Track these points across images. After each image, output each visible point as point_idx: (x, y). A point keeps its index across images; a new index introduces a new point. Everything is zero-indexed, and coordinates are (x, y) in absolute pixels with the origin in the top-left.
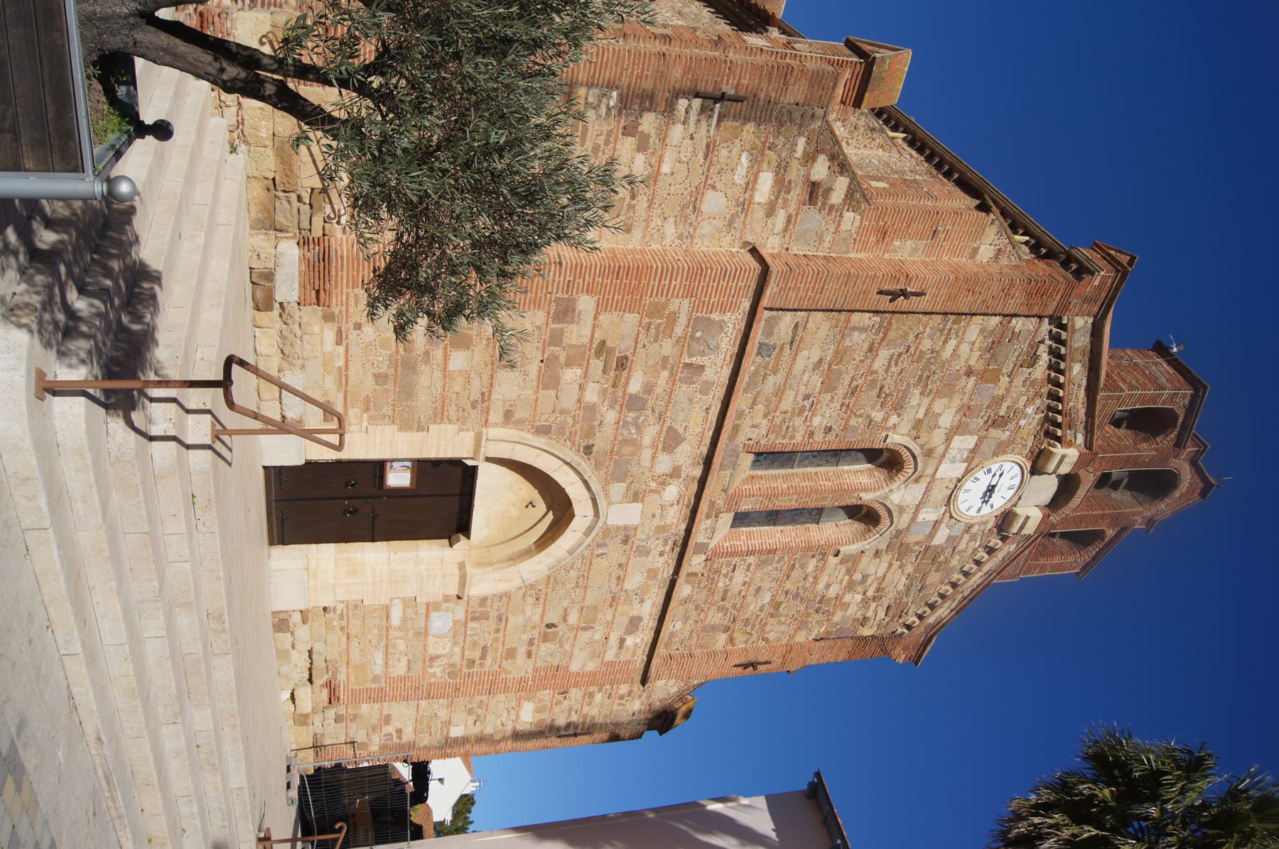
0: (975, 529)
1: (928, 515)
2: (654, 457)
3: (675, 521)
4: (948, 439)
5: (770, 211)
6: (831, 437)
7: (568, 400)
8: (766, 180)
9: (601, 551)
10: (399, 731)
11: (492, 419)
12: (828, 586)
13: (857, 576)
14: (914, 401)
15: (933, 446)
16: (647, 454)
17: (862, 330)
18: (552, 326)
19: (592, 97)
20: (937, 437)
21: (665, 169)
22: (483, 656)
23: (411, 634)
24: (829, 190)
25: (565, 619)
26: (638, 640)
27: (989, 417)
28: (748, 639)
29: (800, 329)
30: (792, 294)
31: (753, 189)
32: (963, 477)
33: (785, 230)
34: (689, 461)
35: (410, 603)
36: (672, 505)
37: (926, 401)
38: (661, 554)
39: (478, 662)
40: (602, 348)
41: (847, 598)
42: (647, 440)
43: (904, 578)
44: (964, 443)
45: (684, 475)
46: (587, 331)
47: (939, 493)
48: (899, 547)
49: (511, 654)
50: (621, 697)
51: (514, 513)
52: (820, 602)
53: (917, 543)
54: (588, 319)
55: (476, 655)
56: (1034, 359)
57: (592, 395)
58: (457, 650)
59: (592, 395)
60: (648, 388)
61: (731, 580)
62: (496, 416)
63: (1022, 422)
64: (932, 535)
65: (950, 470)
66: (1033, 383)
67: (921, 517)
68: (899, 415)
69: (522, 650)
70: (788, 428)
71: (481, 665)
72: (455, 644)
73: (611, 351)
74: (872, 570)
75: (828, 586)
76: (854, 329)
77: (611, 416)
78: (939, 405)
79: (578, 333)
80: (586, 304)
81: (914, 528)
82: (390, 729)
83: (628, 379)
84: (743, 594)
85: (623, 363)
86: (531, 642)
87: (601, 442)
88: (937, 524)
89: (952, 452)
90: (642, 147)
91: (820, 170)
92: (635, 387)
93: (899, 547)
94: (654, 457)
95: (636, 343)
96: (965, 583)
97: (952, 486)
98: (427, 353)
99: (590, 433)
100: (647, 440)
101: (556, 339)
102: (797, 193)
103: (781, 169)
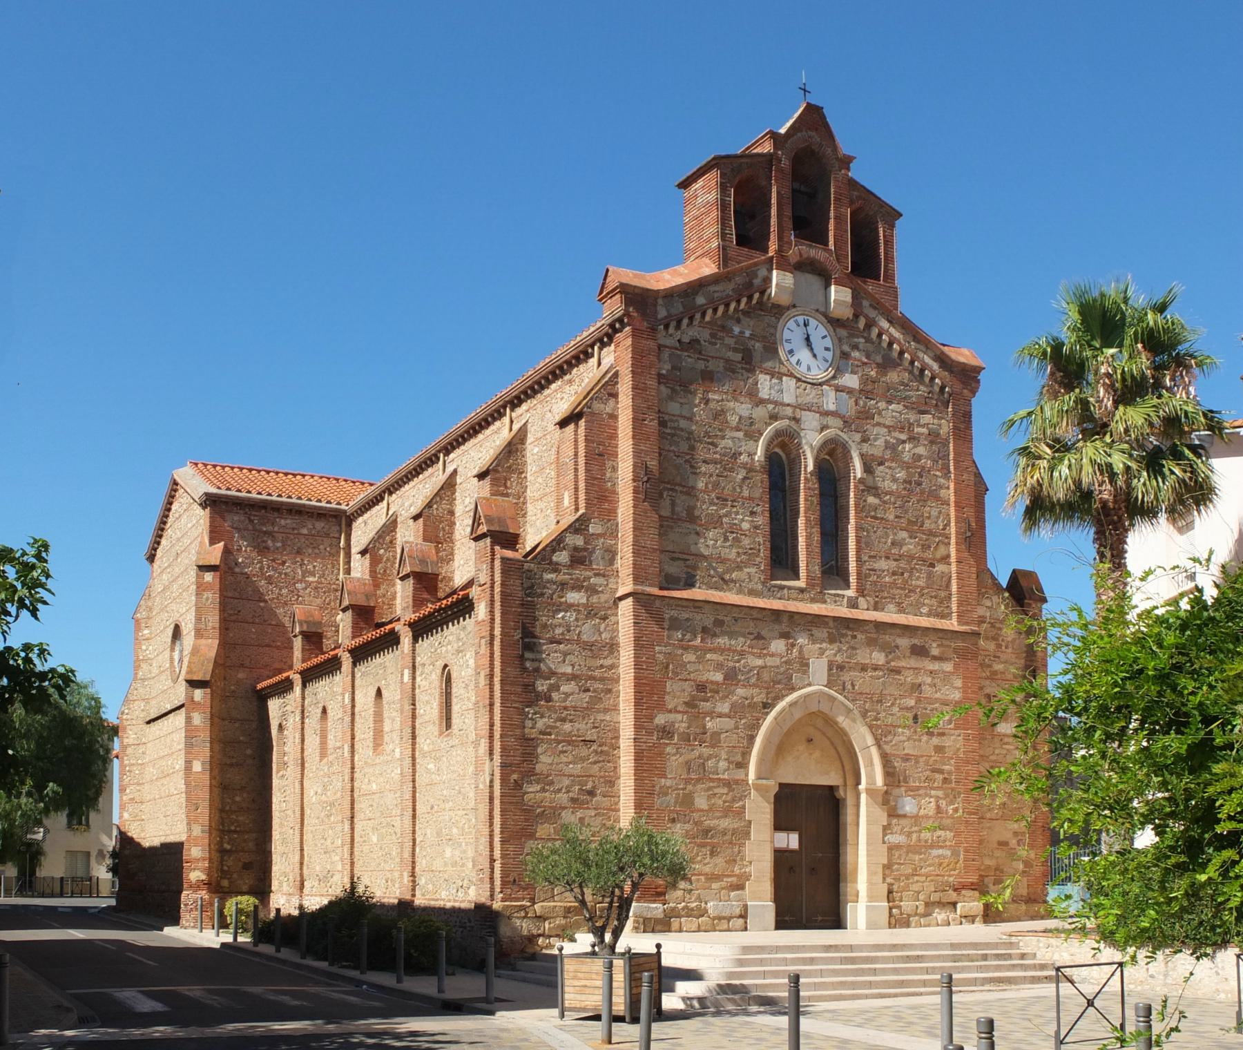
0: (846, 348)
1: (830, 401)
2: (772, 655)
3: (825, 630)
4: (762, 402)
5: (592, 590)
6: (759, 509)
7: (728, 723)
8: (573, 597)
9: (849, 687)
10: (1016, 834)
11: (743, 777)
12: (894, 480)
13: (888, 455)
14: (729, 443)
15: (767, 415)
16: (770, 661)
17: (673, 504)
18: (676, 741)
19: (529, 723)
20: (760, 413)
21: (569, 670)
22: (941, 772)
23: (916, 829)
24: (576, 549)
25: (909, 709)
26: (934, 645)
27: (742, 368)
28: (943, 543)
29: (674, 555)
30: (651, 570)
31: (578, 605)
32: (795, 377)
33: (604, 576)
34: (776, 627)
35: (886, 829)
36: (812, 635)
37: (729, 434)
38: (854, 637)
39: (946, 776)
40: (690, 704)
41: (906, 457)
42: (759, 662)
43: (892, 407)
44: (765, 386)
45: (788, 629)
46: (679, 717)
47: (810, 396)
48: (860, 420)
49: (939, 749)
50: (999, 646)
51: (817, 754)
52: (910, 483)
53: (857, 404)
54: (672, 716)
55: (940, 777)
56: (694, 342)
57: (724, 707)
58: (933, 792)
59: (724, 707)
60: (719, 666)
61: (884, 571)
62: (739, 775)
63: (747, 333)
64: (850, 391)
65: (789, 391)
66: (713, 335)
67: (832, 407)
68: (740, 454)
69: (935, 741)
70: (751, 549)
71: (950, 773)
72: (926, 795)
73: (693, 698)
74: (880, 442)
75: (894, 480)
76: (673, 512)
77: (741, 691)
78: (733, 420)
79: (680, 722)
80: (660, 719)
81: (843, 411)
82: (1013, 842)
83: (712, 682)
84: (897, 557)
85: (701, 687)
86: (930, 734)
87: (760, 698)
88: (838, 389)
89: (775, 395)
90: (556, 688)
91: (562, 557)
92: (719, 677)
93: (860, 420)
94: (772, 655)
95: (686, 680)
96: (899, 344)
97: (804, 385)
98: (696, 823)
99: (752, 706)
100: (759, 662)
101: (686, 738)
102: (578, 573)
103: (563, 586)
